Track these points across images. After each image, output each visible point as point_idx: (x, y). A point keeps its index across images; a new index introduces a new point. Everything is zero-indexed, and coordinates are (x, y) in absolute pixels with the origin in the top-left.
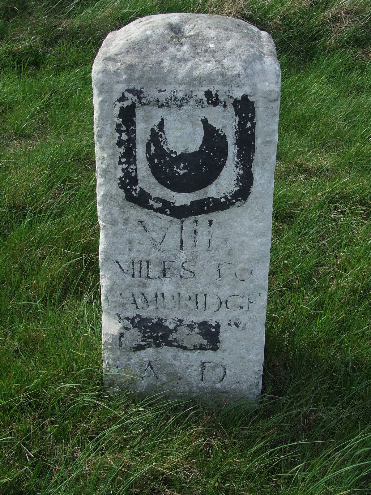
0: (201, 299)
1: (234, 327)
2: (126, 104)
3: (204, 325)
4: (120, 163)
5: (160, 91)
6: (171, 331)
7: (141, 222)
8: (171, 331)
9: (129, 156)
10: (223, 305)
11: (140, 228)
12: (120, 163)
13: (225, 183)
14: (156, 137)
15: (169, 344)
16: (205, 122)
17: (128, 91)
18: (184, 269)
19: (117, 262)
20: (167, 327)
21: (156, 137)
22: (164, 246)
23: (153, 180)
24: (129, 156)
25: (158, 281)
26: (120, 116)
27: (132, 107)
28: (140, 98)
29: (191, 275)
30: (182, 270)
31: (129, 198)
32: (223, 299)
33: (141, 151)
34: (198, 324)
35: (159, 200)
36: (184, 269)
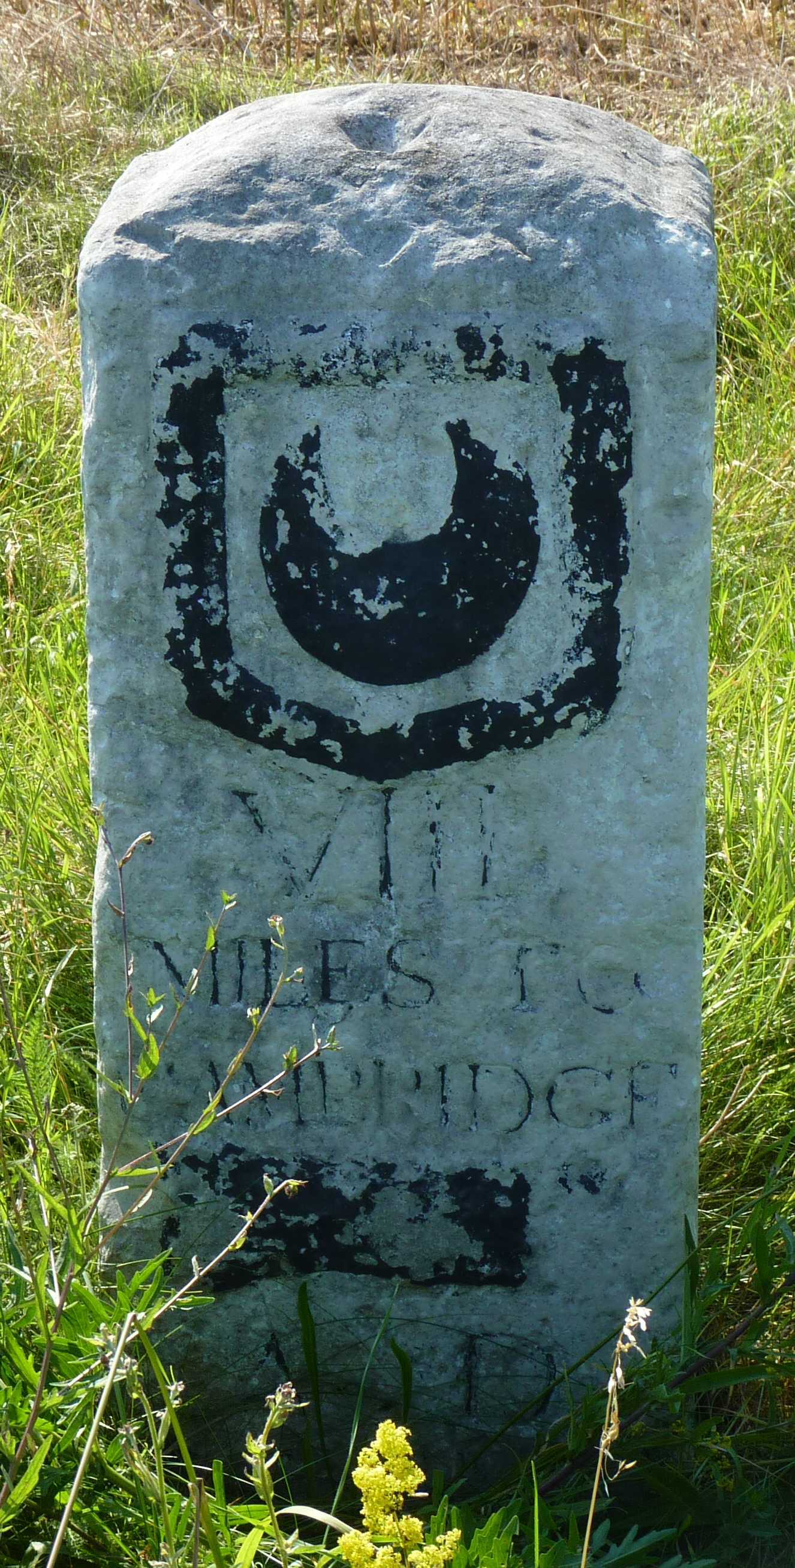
0: (458, 1082)
1: (580, 1191)
2: (189, 374)
3: (469, 1184)
4: (172, 580)
5: (307, 329)
6: (351, 1209)
7: (244, 796)
8: (351, 1209)
9: (202, 556)
10: (539, 1106)
11: (239, 817)
12: (172, 580)
13: (530, 652)
14: (291, 488)
15: (343, 1260)
16: (459, 432)
17: (197, 329)
18: (396, 968)
19: (158, 946)
20: (336, 1193)
21: (291, 488)
22: (324, 883)
23: (286, 642)
24: (202, 556)
25: (304, 1014)
26: (173, 417)
27: (215, 383)
28: (239, 355)
29: (418, 992)
30: (391, 974)
31: (203, 704)
32: (539, 1084)
33: (241, 540)
34: (448, 1178)
35: (306, 711)
36: (396, 968)
